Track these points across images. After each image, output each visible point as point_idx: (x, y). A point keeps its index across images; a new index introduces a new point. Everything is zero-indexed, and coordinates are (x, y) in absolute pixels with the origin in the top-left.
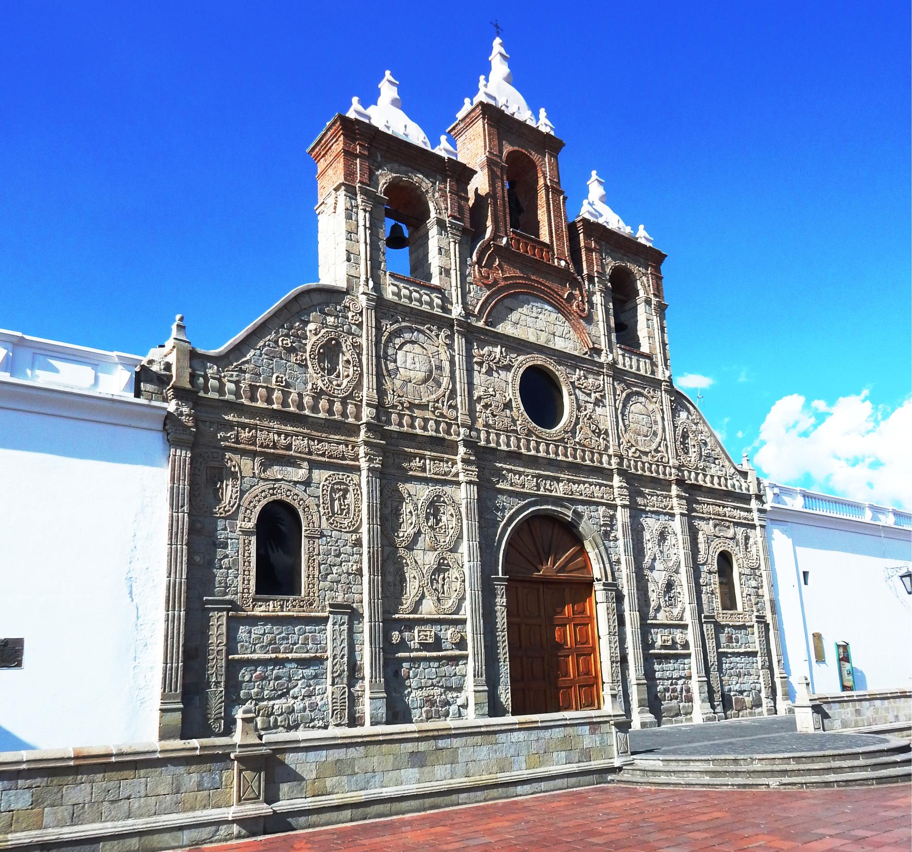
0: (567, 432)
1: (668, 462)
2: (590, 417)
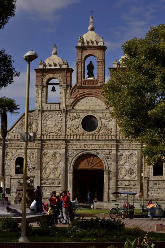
0: (97, 132)
2: (106, 126)
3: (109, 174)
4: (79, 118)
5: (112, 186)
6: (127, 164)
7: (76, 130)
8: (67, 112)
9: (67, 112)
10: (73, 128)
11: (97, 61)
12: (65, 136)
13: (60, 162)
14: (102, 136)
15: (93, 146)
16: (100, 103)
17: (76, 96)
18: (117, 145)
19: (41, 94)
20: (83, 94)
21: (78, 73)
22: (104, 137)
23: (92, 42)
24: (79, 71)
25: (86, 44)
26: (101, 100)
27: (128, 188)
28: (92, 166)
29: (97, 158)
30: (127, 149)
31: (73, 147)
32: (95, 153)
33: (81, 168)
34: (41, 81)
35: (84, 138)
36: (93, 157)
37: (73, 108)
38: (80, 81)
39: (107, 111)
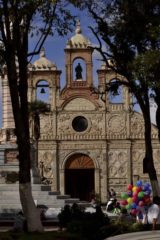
1: (126, 133)
2: (96, 126)
3: (100, 173)
4: (69, 119)
5: (103, 185)
6: (117, 162)
7: (66, 131)
8: (57, 113)
9: (57, 113)
10: (64, 128)
11: (86, 63)
12: (56, 136)
13: (51, 162)
14: (92, 136)
15: (83, 145)
16: (90, 104)
17: (66, 97)
18: (107, 144)
19: (31, 96)
20: (72, 95)
21: (67, 75)
22: (94, 137)
23: (81, 45)
24: (68, 73)
25: (74, 47)
26: (90, 101)
27: (119, 186)
28: (83, 165)
29: (88, 157)
30: (117, 149)
31: (64, 147)
32: (85, 153)
33: (72, 167)
34: (31, 83)
35: (75, 139)
36: (83, 157)
37: (63, 109)
38: (69, 83)
39: (97, 112)
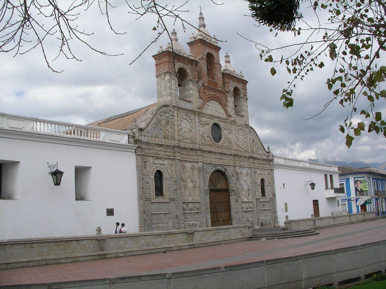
39: (228, 121)
